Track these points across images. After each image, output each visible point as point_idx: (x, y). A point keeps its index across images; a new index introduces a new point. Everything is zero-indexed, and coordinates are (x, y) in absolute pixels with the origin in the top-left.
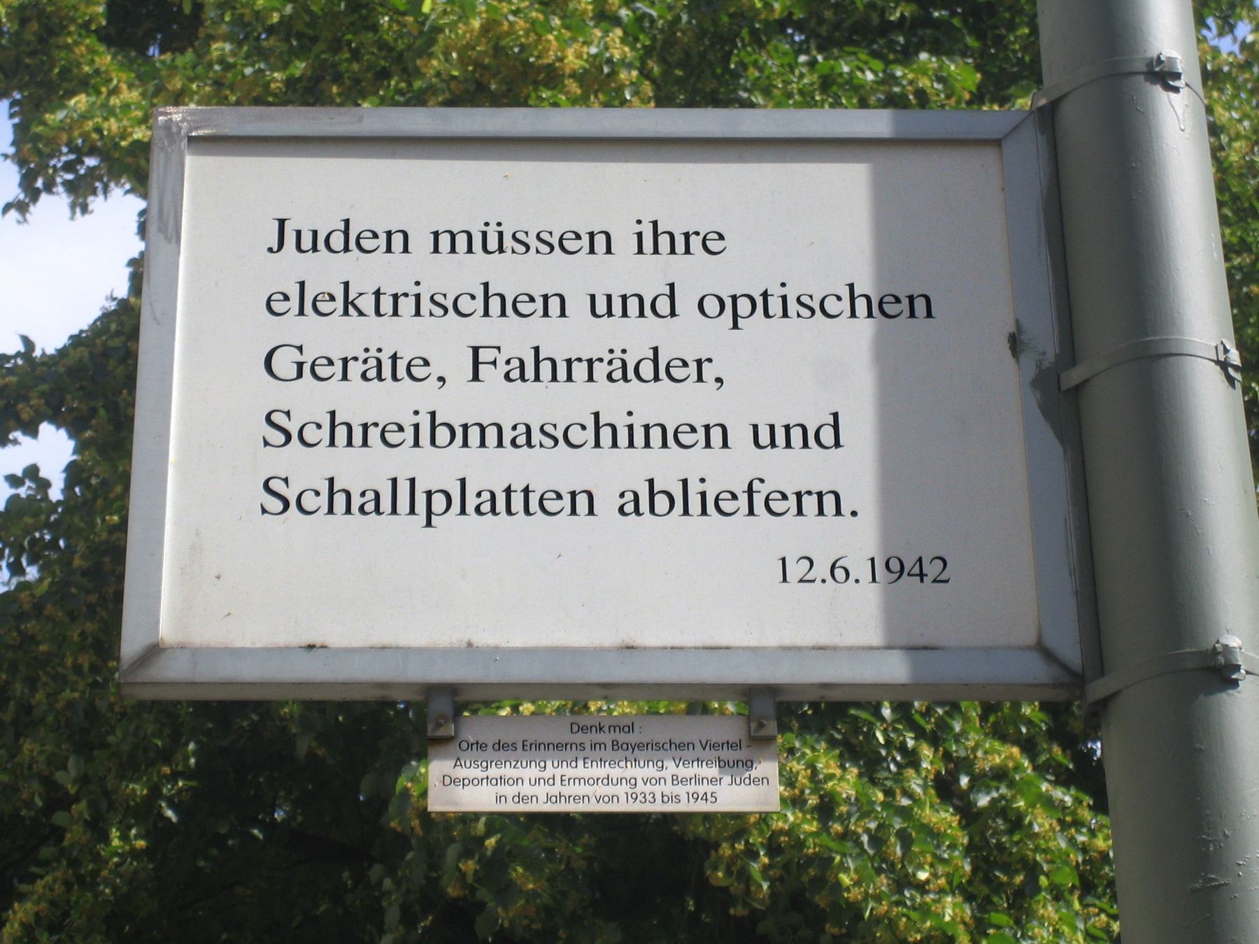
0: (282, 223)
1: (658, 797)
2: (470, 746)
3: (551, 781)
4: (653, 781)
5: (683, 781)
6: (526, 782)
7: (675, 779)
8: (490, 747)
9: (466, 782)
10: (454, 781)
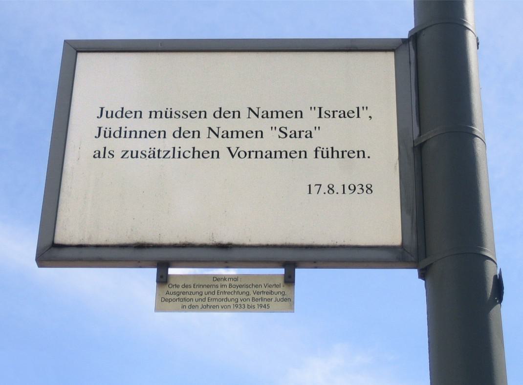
0: (100, 128)
1: (246, 306)
2: (173, 286)
3: (204, 300)
4: (245, 300)
5: (257, 300)
6: (194, 300)
7: (253, 299)
8: (181, 287)
9: (170, 300)
10: (166, 300)
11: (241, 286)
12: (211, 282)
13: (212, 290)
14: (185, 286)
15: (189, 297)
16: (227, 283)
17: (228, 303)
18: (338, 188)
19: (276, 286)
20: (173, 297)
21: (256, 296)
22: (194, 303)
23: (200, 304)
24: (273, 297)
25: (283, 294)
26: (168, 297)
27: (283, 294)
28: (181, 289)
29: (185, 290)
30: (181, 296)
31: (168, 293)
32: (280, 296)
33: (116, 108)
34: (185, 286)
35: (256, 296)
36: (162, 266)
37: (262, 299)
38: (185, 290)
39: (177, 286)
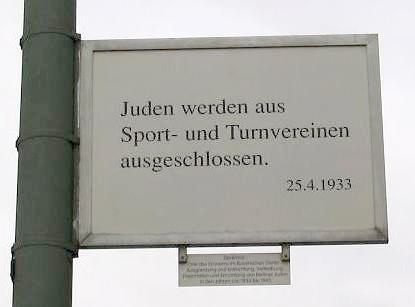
11: (247, 263)
12: (222, 261)
13: (223, 267)
14: (202, 264)
15: (205, 273)
16: (235, 261)
17: (237, 278)
18: (318, 184)
19: (276, 263)
20: (193, 273)
21: (260, 272)
22: (210, 279)
23: (215, 279)
24: (274, 272)
25: (281, 269)
26: (188, 274)
27: (281, 269)
28: (197, 267)
29: (202, 267)
30: (199, 273)
31: (188, 270)
32: (279, 272)
33: (143, 104)
34: (202, 264)
35: (260, 272)
36: (182, 247)
37: (265, 275)
38: (202, 267)
39: (195, 265)
